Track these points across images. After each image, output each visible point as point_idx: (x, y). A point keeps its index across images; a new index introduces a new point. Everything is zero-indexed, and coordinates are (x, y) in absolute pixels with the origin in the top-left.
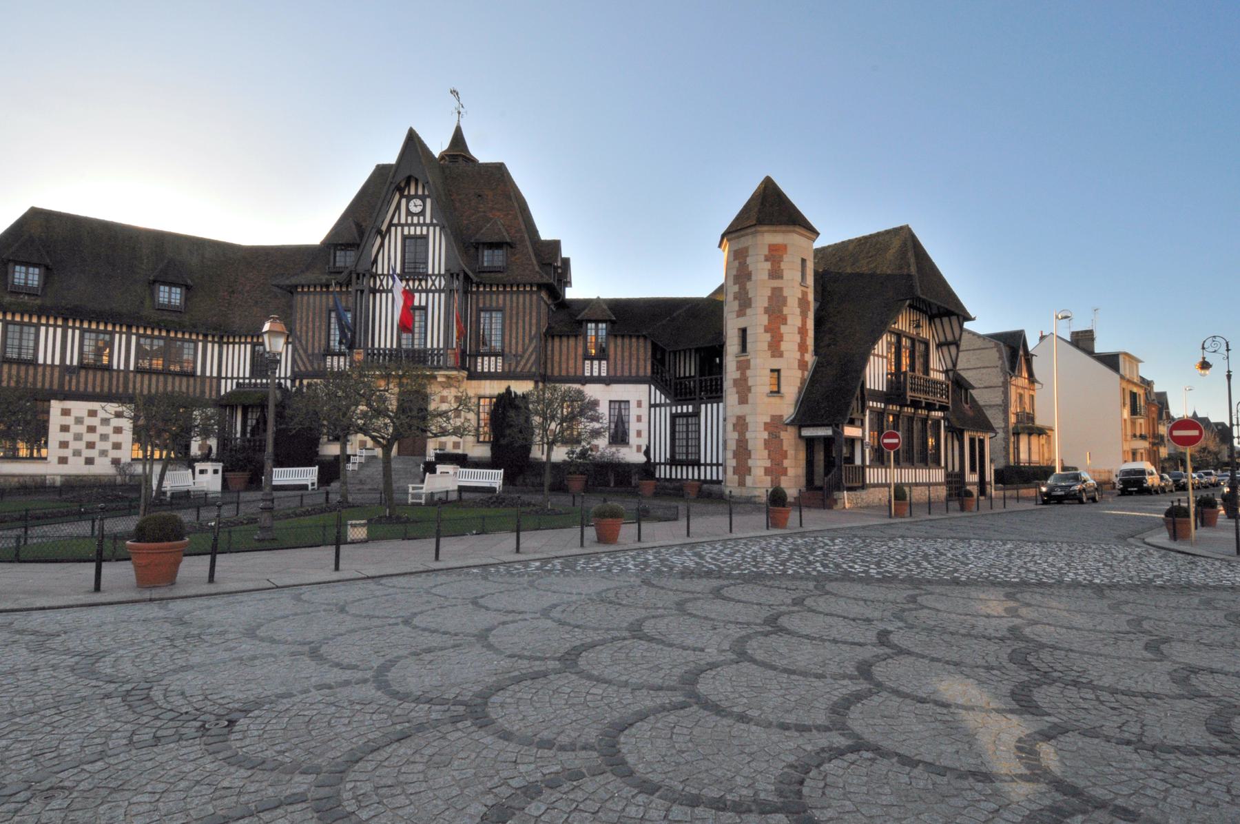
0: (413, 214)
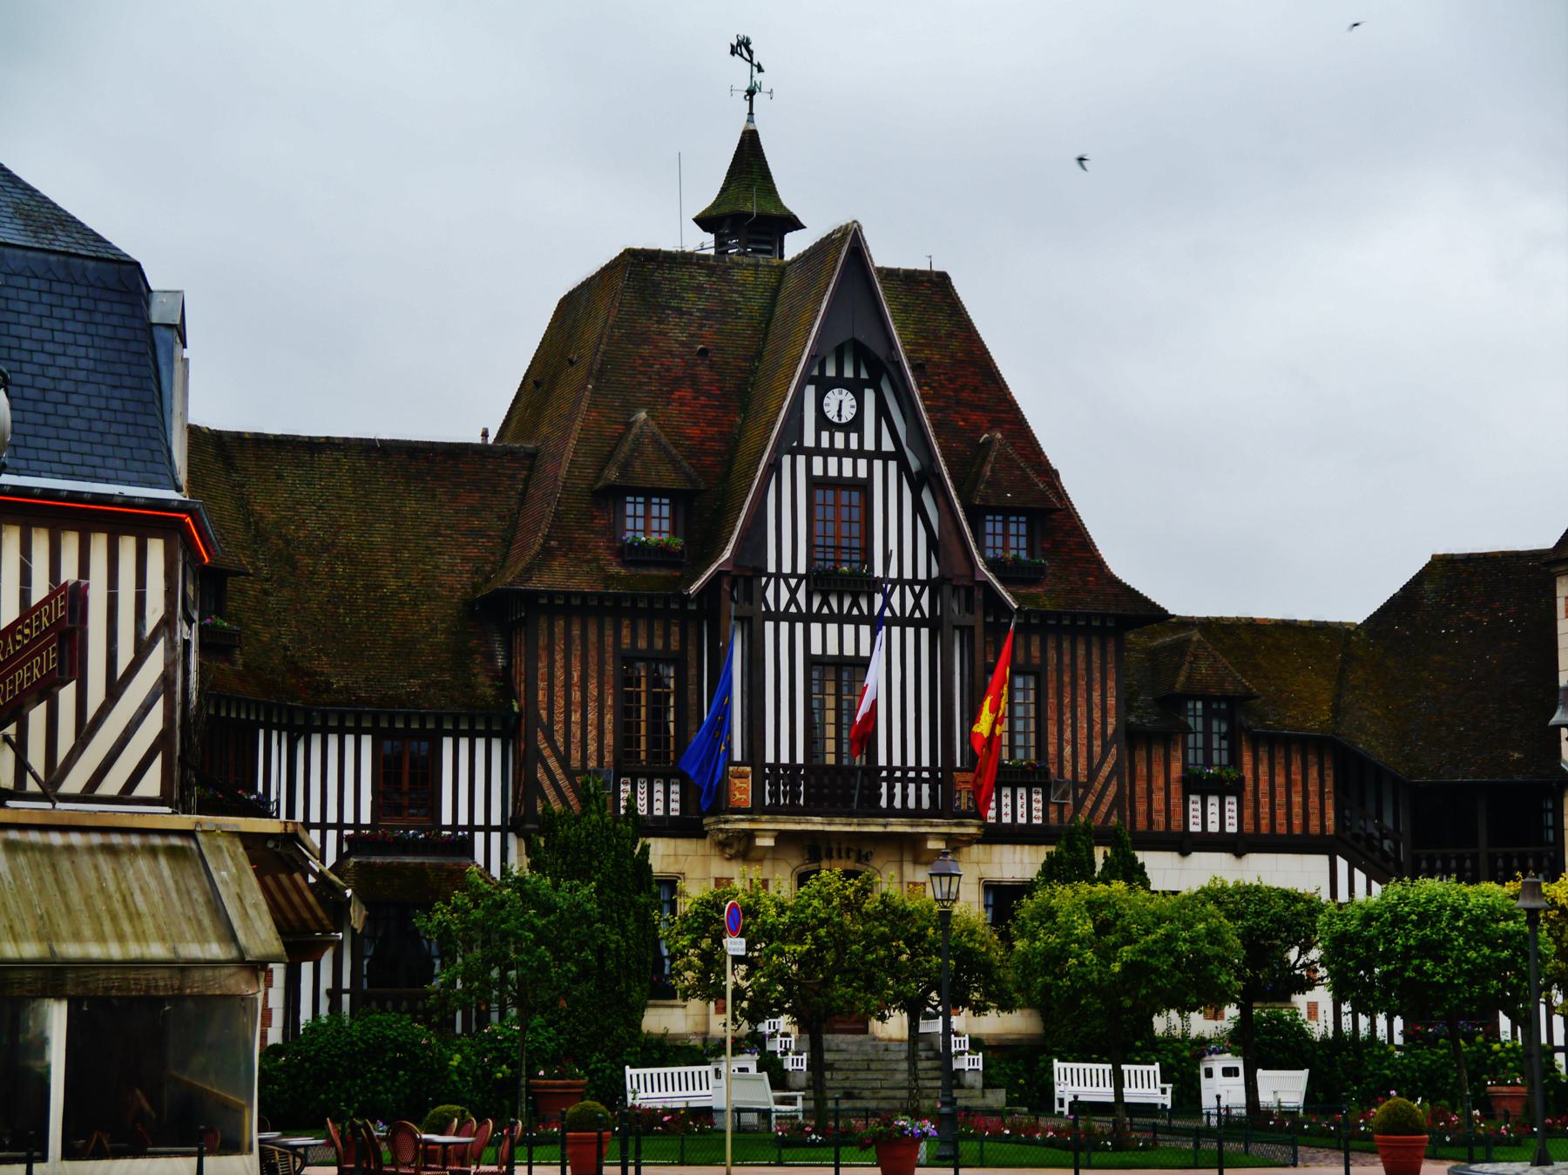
0: (832, 427)
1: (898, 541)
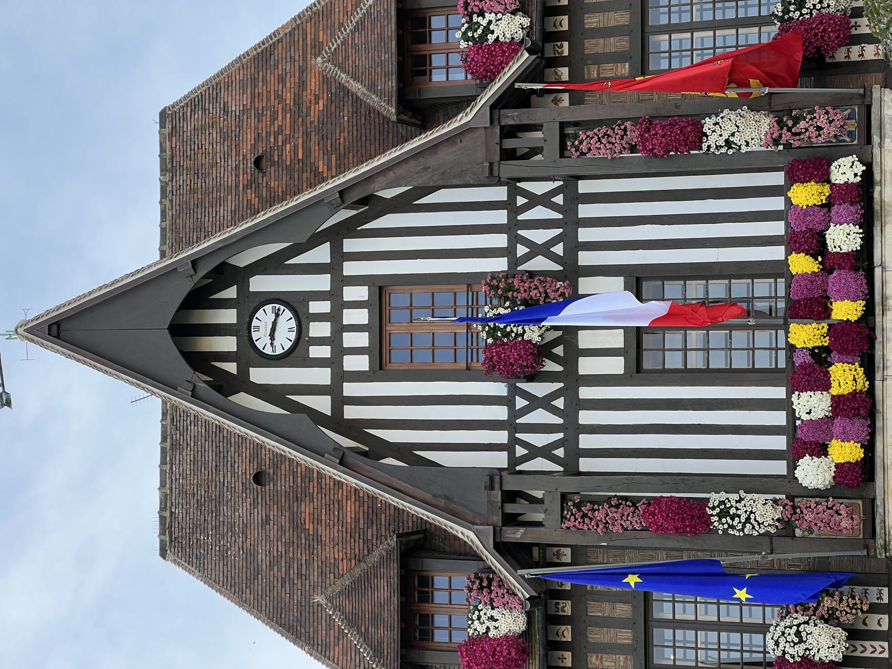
0: (302, 340)
1: (453, 236)
